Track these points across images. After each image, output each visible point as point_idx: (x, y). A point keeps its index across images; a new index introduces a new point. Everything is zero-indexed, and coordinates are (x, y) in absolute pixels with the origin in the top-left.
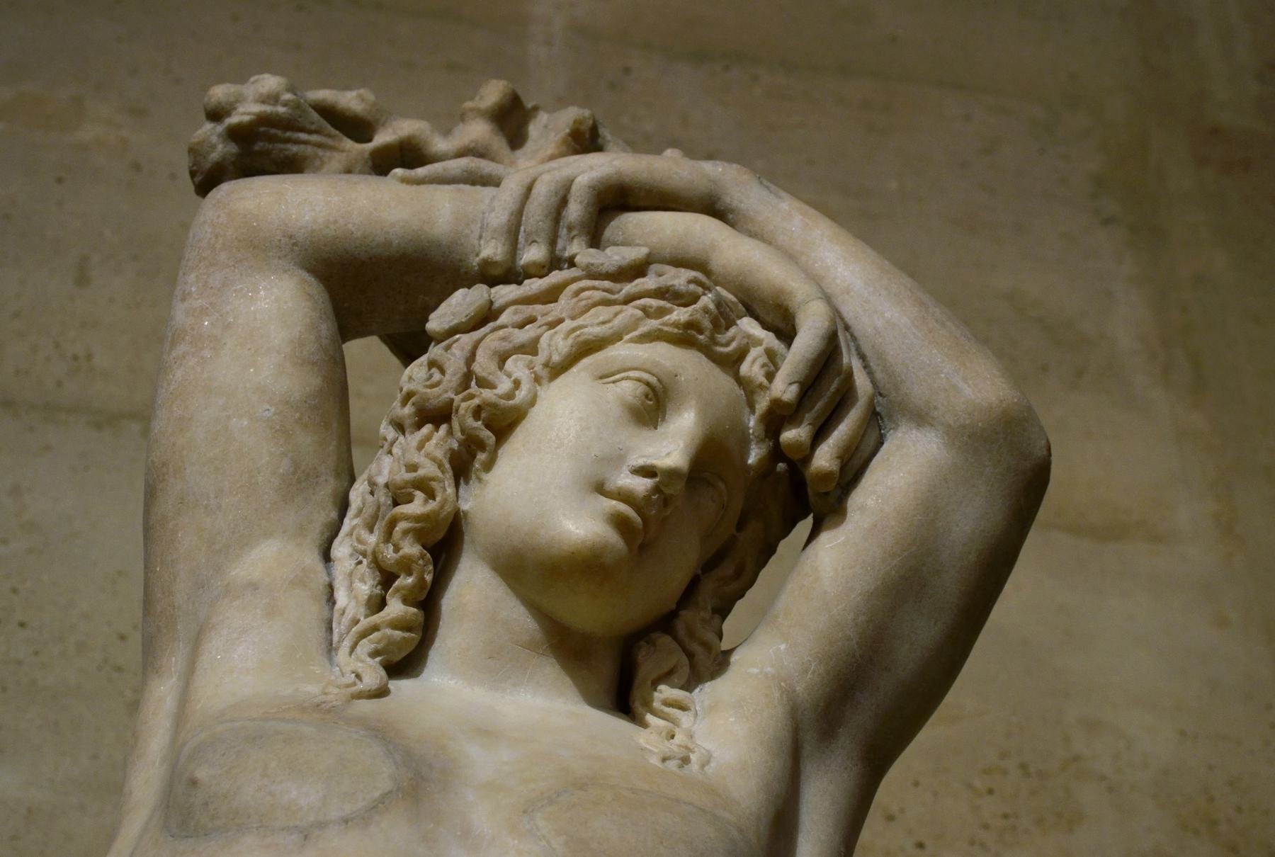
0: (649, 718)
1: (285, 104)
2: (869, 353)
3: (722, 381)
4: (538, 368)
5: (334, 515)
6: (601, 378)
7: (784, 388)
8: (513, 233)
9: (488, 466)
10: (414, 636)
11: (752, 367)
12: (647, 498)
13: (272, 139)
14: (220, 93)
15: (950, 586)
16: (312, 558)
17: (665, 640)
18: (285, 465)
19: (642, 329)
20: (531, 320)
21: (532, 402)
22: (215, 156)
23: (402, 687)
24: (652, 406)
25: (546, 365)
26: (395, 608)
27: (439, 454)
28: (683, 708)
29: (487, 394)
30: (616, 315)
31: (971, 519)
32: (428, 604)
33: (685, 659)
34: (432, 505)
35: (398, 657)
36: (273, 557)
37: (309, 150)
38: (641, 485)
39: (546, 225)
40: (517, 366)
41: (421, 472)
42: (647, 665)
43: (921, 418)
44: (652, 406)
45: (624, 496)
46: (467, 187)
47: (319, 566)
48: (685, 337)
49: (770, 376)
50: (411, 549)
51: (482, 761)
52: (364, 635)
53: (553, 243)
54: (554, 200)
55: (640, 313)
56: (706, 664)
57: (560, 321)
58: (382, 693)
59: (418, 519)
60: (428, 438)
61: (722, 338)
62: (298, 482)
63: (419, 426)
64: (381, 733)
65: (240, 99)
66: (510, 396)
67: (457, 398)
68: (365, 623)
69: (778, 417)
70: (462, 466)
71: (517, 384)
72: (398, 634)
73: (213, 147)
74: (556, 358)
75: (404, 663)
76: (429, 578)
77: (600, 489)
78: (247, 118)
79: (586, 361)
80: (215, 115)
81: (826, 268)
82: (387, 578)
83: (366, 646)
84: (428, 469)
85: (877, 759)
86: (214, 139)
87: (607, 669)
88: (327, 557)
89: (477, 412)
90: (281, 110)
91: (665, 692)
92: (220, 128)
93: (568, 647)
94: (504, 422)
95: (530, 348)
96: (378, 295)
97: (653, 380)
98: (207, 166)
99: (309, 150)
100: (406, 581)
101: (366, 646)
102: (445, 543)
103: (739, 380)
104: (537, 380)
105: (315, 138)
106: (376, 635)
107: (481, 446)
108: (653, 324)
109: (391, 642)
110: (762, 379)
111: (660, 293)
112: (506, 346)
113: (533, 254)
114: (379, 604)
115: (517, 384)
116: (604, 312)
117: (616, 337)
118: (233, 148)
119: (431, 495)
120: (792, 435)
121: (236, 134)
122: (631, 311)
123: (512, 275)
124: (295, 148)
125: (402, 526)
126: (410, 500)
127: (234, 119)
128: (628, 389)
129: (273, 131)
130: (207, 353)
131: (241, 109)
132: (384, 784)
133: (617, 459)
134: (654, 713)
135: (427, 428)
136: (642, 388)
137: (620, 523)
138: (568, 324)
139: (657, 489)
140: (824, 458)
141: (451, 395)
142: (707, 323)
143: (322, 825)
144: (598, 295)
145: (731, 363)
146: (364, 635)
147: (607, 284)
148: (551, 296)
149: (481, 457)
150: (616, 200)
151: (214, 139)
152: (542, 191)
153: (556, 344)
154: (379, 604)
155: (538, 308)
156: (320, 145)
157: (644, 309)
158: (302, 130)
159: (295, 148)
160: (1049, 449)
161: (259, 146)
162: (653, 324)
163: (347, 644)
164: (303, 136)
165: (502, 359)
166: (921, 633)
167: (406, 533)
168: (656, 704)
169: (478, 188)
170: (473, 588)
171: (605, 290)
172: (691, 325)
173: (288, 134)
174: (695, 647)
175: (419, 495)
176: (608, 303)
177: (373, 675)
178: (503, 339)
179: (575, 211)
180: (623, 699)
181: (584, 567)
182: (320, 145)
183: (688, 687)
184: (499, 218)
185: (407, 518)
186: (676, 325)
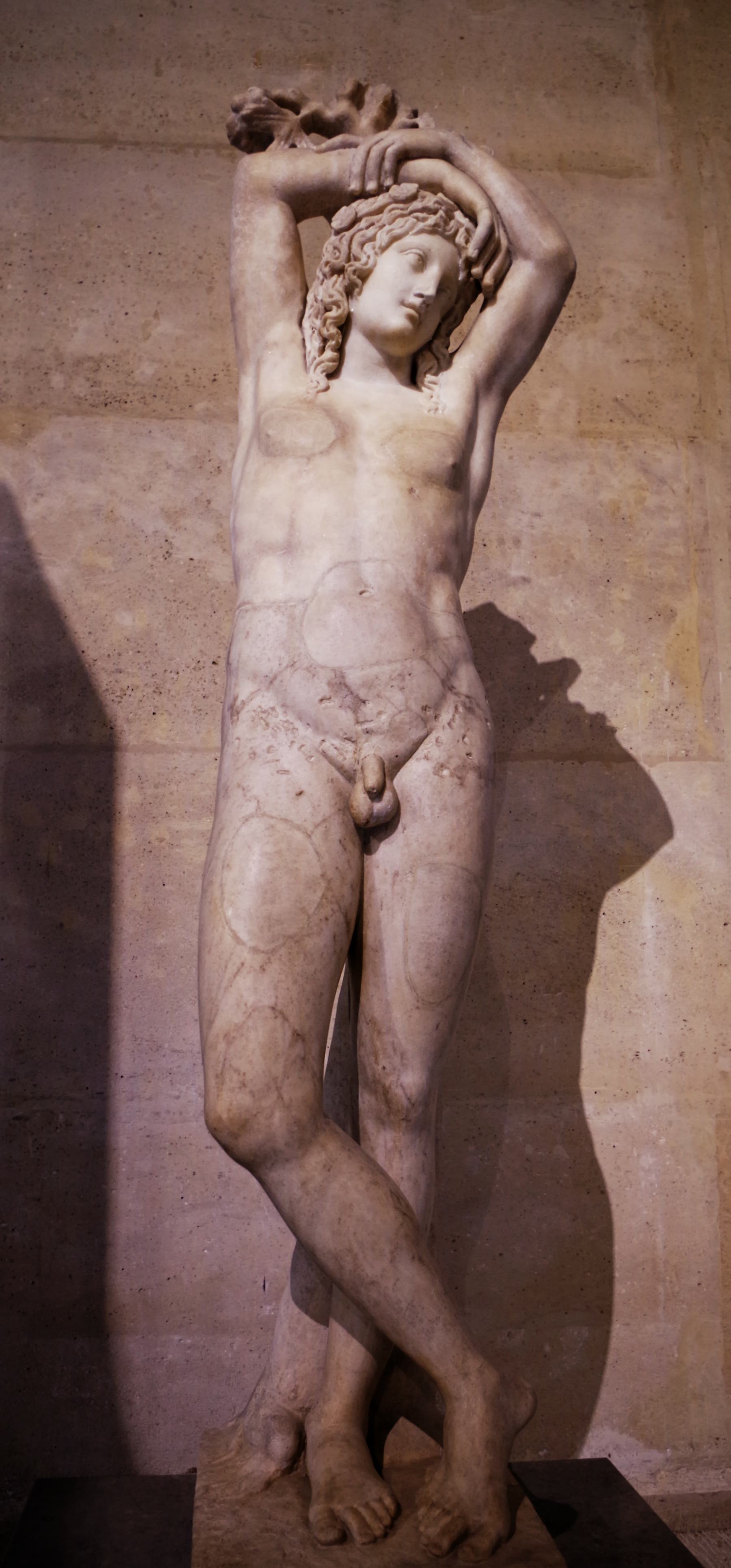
0: (423, 388)
1: (264, 103)
2: (507, 225)
3: (448, 247)
4: (377, 249)
5: (302, 308)
6: (402, 252)
7: (472, 251)
8: (363, 177)
9: (360, 293)
10: (336, 364)
11: (460, 239)
12: (420, 307)
13: (260, 119)
14: (237, 99)
15: (535, 327)
16: (295, 328)
17: (428, 355)
18: (282, 291)
19: (416, 229)
20: (372, 224)
21: (375, 265)
22: (237, 129)
23: (334, 383)
24: (421, 264)
25: (380, 248)
26: (329, 354)
27: (341, 289)
28: (435, 383)
29: (357, 265)
30: (406, 222)
31: (543, 299)
32: (340, 350)
33: (436, 362)
34: (340, 311)
35: (331, 371)
36: (282, 329)
37: (275, 123)
38: (418, 301)
39: (376, 172)
40: (368, 247)
41: (334, 299)
42: (422, 367)
43: (526, 256)
44: (421, 264)
45: (412, 307)
46: (341, 151)
47: (299, 332)
48: (434, 230)
49: (467, 241)
50: (333, 330)
51: (366, 421)
52: (318, 364)
53: (379, 178)
54: (379, 160)
55: (415, 220)
56: (444, 362)
57: (384, 225)
58: (327, 389)
59: (335, 318)
60: (336, 282)
62: (287, 298)
63: (332, 275)
64: (329, 412)
65: (245, 101)
66: (366, 264)
67: (347, 265)
68: (318, 359)
69: (470, 263)
70: (350, 292)
71: (369, 257)
72: (331, 364)
73: (236, 125)
74: (384, 244)
75: (333, 374)
76: (340, 341)
77: (402, 303)
78: (248, 111)
79: (395, 244)
80: (236, 109)
81: (489, 183)
82: (325, 340)
83: (319, 369)
84: (337, 297)
85: (506, 395)
86: (236, 121)
87: (407, 369)
88: (300, 324)
89: (354, 272)
90: (262, 105)
91: (429, 377)
92: (239, 116)
93: (392, 363)
94: (364, 276)
95: (373, 239)
96: (310, 204)
97: (421, 253)
98: (235, 133)
99: (275, 123)
100: (332, 343)
101: (319, 369)
102: (345, 325)
103: (455, 245)
104: (376, 254)
105: (277, 116)
106: (322, 365)
107: (356, 285)
108: (421, 225)
109: (328, 367)
110: (464, 244)
111: (424, 210)
112: (363, 239)
113: (371, 186)
114: (322, 350)
115: (369, 257)
116: (400, 221)
117: (406, 233)
118: (244, 125)
119: (339, 307)
120: (476, 270)
121: (246, 119)
122: (411, 220)
123: (364, 195)
124: (269, 122)
125: (329, 321)
126: (330, 310)
127: (244, 112)
128: (412, 258)
129: (261, 116)
130: (248, 242)
131: (246, 107)
132: (333, 437)
133: (408, 290)
134: (425, 386)
135: (336, 276)
136: (417, 257)
137: (410, 318)
138: (387, 228)
139: (424, 302)
140: (488, 279)
141: (343, 263)
142: (442, 224)
143: (314, 455)
144: (398, 212)
145: (451, 238)
146: (318, 364)
147: (401, 206)
148: (380, 211)
149: (357, 290)
150: (405, 156)
151: (236, 121)
152: (374, 154)
153: (382, 237)
154: (322, 350)
155: (375, 218)
156: (279, 120)
157: (417, 218)
158: (271, 113)
159: (269, 122)
160: (576, 266)
161: (255, 123)
162: (421, 225)
163: (312, 368)
164: (272, 116)
165: (362, 245)
166: (525, 345)
167: (330, 324)
168: (426, 383)
169: (347, 150)
170: (356, 342)
171: (402, 209)
172: (436, 225)
173: (266, 116)
174: (440, 357)
175: (334, 308)
176: (402, 216)
177: (323, 382)
178: (363, 236)
179: (387, 165)
180: (413, 380)
181: (398, 337)
182: (279, 120)
183: (436, 374)
184: (356, 169)
185: (331, 318)
186: (430, 226)
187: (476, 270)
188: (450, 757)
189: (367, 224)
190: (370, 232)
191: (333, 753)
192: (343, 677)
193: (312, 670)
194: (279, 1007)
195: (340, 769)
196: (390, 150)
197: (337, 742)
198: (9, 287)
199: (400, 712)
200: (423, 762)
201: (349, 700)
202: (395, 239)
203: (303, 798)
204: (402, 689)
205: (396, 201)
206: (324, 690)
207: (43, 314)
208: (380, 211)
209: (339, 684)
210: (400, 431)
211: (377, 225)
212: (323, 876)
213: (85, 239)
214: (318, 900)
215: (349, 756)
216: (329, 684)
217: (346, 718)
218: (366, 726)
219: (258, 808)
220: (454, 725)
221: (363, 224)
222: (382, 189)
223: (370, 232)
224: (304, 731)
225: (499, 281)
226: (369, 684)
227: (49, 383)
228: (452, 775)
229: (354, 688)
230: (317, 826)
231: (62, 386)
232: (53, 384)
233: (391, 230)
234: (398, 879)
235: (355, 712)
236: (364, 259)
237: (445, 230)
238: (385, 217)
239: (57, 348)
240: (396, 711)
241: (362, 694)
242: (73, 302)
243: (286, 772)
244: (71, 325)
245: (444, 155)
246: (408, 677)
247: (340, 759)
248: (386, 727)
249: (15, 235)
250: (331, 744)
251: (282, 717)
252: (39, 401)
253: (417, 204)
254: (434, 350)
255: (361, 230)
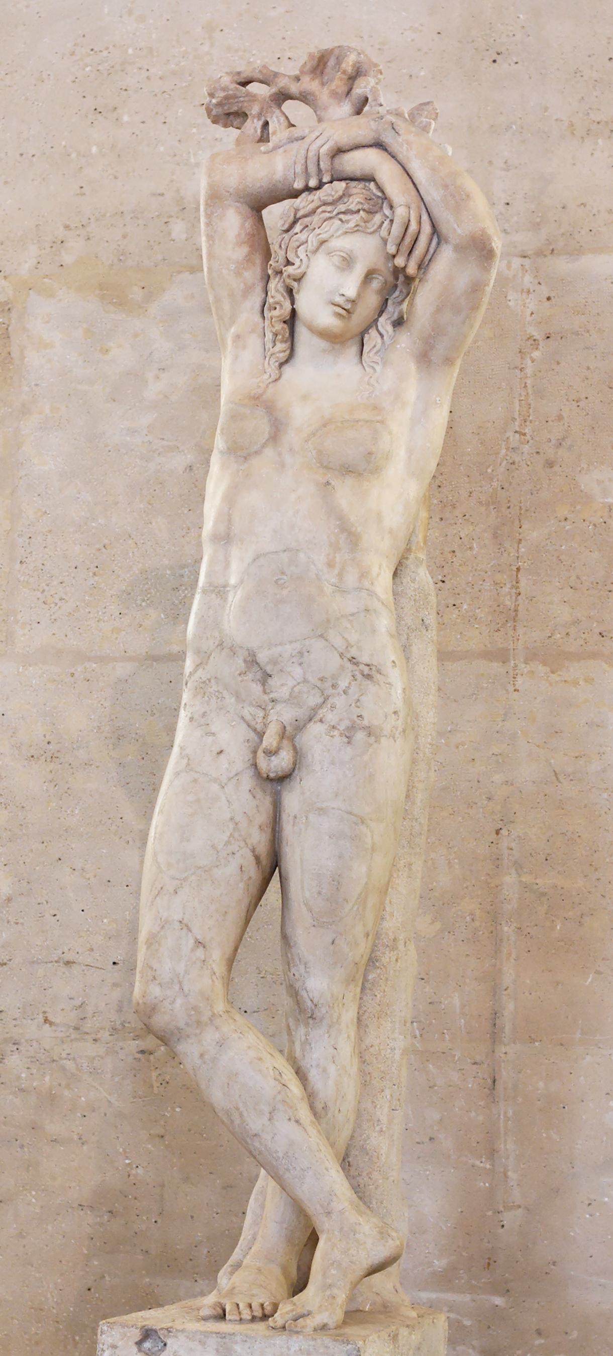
5: (264, 296)
9: (298, 292)
16: (257, 318)
21: (308, 267)
23: (287, 369)
26: (280, 346)
41: (276, 299)
44: (348, 262)
47: (261, 320)
48: (357, 230)
50: (279, 326)
54: (315, 158)
61: (369, 225)
64: (270, 408)
72: (282, 355)
76: (287, 335)
101: (273, 360)
102: (292, 319)
112: (298, 244)
113: (313, 183)
114: (274, 342)
123: (307, 189)
132: (266, 436)
138: (317, 231)
143: (249, 455)
144: (328, 215)
147: (329, 208)
150: (339, 151)
153: (313, 241)
156: (249, 101)
157: (341, 220)
170: (302, 332)
176: (331, 218)
182: (249, 101)
184: (299, 169)
187: (400, 261)
188: (341, 720)
189: (302, 227)
190: (302, 237)
191: (248, 717)
192: (255, 656)
193: (233, 651)
194: (185, 921)
195: (255, 730)
196: (323, 151)
197: (252, 710)
198: (126, 118)
199: (299, 683)
200: (319, 724)
201: (259, 675)
202: (323, 242)
203: (222, 756)
204: (300, 664)
205: (325, 204)
206: (240, 663)
207: (162, 149)
208: (314, 212)
209: (252, 661)
210: (325, 425)
211: (311, 227)
212: (231, 819)
213: (206, 48)
214: (226, 839)
215: (260, 720)
216: (245, 661)
217: (257, 688)
218: (272, 696)
219: (188, 765)
220: (350, 691)
221: (298, 228)
222: (319, 187)
223: (302, 237)
224: (230, 700)
225: (423, 266)
226: (274, 662)
227: (170, 234)
228: (341, 735)
229: (262, 664)
230: (230, 779)
231: (184, 236)
232: (174, 235)
233: (319, 234)
234: (297, 820)
235: (263, 685)
236: (297, 262)
237: (366, 227)
238: (316, 219)
239: (178, 191)
240: (295, 683)
241: (269, 669)
242: (194, 130)
243: (213, 734)
244: (192, 160)
245: (379, 145)
246: (306, 654)
247: (253, 723)
248: (287, 696)
249: (130, 51)
250: (247, 711)
251: (215, 688)
252: (160, 257)
253: (342, 207)
254: (380, 328)
255: (297, 234)
